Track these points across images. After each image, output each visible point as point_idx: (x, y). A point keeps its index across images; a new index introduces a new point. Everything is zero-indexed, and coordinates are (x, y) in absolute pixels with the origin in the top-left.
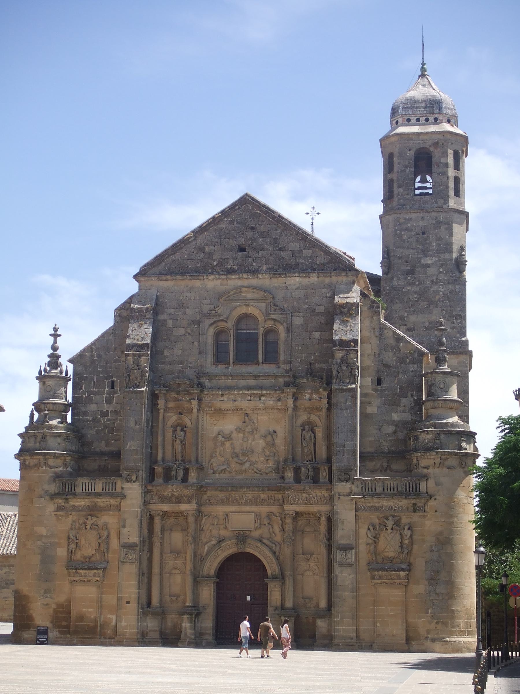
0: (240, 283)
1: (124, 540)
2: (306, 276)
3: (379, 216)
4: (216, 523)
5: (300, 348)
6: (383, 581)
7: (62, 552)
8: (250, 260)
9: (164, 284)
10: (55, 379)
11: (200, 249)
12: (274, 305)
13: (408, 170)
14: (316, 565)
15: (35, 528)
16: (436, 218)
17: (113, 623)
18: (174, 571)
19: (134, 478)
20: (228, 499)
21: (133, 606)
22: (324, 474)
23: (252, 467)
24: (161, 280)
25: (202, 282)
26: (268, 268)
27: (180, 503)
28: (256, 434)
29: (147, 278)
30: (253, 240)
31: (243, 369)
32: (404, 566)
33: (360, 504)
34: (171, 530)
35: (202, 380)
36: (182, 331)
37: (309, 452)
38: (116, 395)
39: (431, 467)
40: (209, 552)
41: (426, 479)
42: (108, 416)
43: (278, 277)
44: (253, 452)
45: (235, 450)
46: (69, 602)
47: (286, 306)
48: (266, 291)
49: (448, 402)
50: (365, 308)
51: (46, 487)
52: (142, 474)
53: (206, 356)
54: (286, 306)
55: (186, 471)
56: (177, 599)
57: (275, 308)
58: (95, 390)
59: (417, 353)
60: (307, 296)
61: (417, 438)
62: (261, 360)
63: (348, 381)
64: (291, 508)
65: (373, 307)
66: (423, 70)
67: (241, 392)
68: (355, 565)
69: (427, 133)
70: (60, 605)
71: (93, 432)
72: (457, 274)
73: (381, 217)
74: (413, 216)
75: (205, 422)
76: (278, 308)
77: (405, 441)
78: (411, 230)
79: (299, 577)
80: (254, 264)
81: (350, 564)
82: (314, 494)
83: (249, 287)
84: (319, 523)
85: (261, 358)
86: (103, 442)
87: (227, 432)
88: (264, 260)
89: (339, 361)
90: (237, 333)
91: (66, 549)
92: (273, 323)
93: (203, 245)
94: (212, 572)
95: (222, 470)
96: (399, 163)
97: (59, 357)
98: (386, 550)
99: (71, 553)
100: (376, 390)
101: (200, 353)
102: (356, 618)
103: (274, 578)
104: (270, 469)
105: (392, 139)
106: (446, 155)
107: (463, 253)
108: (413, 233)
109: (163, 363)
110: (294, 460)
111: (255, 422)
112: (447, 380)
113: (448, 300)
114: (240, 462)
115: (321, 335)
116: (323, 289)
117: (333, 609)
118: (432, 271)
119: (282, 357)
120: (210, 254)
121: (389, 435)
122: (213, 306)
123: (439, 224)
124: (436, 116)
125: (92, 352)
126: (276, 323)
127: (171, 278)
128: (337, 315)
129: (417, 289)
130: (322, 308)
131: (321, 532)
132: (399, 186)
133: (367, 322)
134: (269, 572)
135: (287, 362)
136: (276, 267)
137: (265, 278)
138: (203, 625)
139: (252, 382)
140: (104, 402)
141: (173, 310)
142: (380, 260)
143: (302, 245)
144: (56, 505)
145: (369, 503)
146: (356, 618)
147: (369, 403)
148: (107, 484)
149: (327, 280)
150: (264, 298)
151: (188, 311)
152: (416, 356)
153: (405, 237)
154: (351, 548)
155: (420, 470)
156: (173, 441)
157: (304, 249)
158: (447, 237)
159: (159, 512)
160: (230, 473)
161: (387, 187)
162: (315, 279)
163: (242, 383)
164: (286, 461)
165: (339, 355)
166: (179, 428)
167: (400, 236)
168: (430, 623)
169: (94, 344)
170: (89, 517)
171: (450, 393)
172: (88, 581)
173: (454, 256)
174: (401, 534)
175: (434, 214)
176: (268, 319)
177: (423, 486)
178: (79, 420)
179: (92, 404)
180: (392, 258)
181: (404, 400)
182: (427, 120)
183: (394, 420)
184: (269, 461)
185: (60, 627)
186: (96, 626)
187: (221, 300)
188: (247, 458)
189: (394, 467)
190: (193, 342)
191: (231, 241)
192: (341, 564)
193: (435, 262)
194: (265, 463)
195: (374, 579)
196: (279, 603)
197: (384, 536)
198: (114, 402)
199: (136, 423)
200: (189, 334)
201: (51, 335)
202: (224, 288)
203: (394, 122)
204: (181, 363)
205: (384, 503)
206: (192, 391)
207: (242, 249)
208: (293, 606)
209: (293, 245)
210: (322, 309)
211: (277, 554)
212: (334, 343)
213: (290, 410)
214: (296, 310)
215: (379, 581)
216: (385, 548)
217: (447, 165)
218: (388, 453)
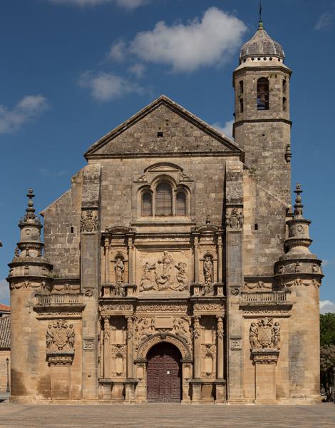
1: (85, 335)
7: (43, 344)
17: (80, 390)
21: (93, 379)
32: (275, 350)
51: (29, 300)
52: (96, 291)
55: (126, 288)
60: (206, 169)
62: (174, 213)
64: (197, 313)
70: (43, 379)
72: (285, 162)
78: (255, 134)
84: (217, 322)
86: (67, 270)
87: (151, 263)
94: (145, 356)
97: (33, 211)
99: (48, 344)
100: (254, 233)
101: (132, 208)
107: (289, 149)
109: (106, 215)
113: (280, 180)
118: (268, 161)
119: (189, 212)
123: (273, 129)
130: (217, 177)
134: (183, 355)
138: (139, 390)
139: (169, 229)
147: (249, 242)
149: (220, 158)
152: (281, 209)
154: (240, 339)
163: (162, 229)
165: (229, 211)
173: (284, 151)
178: (49, 255)
181: (273, 240)
182: (265, 59)
185: (43, 393)
186: (68, 392)
189: (266, 285)
192: (233, 349)
204: (119, 215)
207: (160, 135)
209: (196, 133)
214: (199, 178)
217: (279, 90)
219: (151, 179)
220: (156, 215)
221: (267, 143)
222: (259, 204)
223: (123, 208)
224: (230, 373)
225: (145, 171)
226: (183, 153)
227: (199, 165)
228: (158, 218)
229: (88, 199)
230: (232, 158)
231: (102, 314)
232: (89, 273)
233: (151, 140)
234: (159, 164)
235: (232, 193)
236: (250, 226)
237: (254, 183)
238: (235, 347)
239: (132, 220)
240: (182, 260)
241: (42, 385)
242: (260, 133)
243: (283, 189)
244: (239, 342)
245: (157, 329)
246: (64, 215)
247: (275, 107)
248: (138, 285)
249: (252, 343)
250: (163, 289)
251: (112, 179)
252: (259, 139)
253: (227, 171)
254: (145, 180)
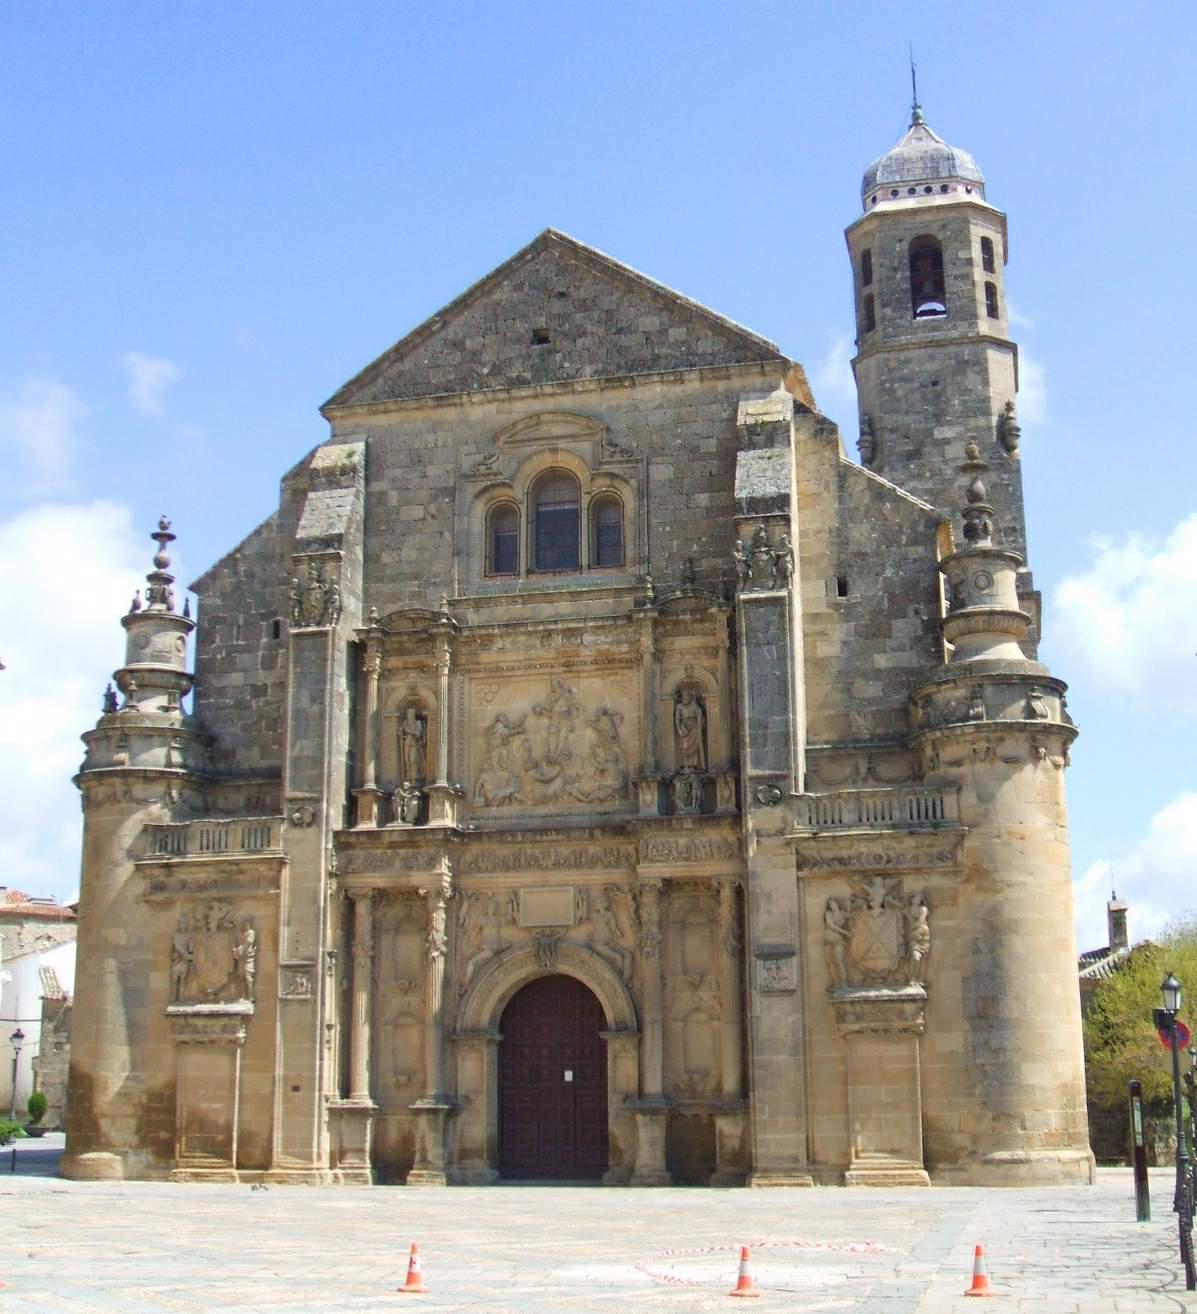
0: (536, 406)
2: (674, 382)
3: (852, 361)
4: (491, 912)
5: (668, 529)
6: (864, 1025)
8: (558, 357)
9: (382, 420)
10: (156, 621)
11: (455, 345)
12: (611, 444)
13: (899, 276)
14: (715, 997)
15: (104, 931)
16: (957, 355)
17: (265, 1136)
18: (403, 1020)
19: (308, 819)
20: (517, 858)
22: (724, 793)
23: (568, 788)
24: (375, 413)
25: (458, 409)
26: (595, 372)
27: (411, 868)
28: (577, 716)
29: (346, 412)
30: (563, 317)
31: (547, 582)
33: (807, 853)
34: (397, 931)
35: (459, 611)
36: (419, 512)
37: (694, 748)
38: (281, 651)
39: (967, 761)
41: (954, 789)
42: (265, 695)
43: (618, 387)
44: (570, 756)
45: (534, 754)
46: (172, 1086)
47: (635, 444)
48: (590, 417)
49: (998, 617)
50: (804, 436)
54: (635, 444)
56: (409, 1079)
57: (613, 449)
58: (241, 643)
59: (923, 521)
60: (679, 421)
61: (928, 700)
62: (584, 561)
63: (771, 584)
64: (653, 871)
65: (822, 430)
66: (916, 117)
67: (541, 628)
68: (799, 992)
69: (930, 209)
70: (154, 1096)
71: (236, 729)
73: (854, 363)
74: (915, 354)
75: (466, 697)
76: (618, 449)
77: (905, 712)
78: (912, 380)
79: (677, 1026)
80: (566, 365)
81: (789, 991)
82: (704, 839)
83: (554, 413)
84: (719, 904)
85: (584, 558)
86: (256, 751)
87: (514, 717)
88: (586, 354)
89: (750, 543)
90: (538, 514)
91: (167, 974)
92: (608, 481)
93: (460, 335)
94: (485, 1018)
95: (504, 798)
96: (881, 265)
97: (169, 580)
98: (871, 955)
100: (837, 606)
102: (805, 1112)
103: (622, 1028)
104: (610, 791)
105: (867, 227)
106: (967, 243)
107: (1011, 414)
108: (916, 385)
110: (658, 767)
112: (991, 569)
114: (541, 778)
115: (711, 499)
116: (714, 403)
117: (751, 1094)
119: (630, 552)
120: (475, 355)
121: (871, 701)
122: (482, 456)
124: (945, 182)
125: (235, 566)
126: (617, 483)
127: (392, 407)
128: (742, 449)
129: (930, 485)
130: (713, 442)
131: (723, 922)
132: (885, 305)
133: (812, 463)
134: (610, 1016)
135: (641, 560)
136: (612, 368)
137: (590, 391)
139: (565, 607)
140: (259, 666)
141: (400, 471)
142: (857, 436)
143: (666, 320)
144: (148, 881)
145: (829, 849)
146: (807, 1113)
148: (252, 832)
149: (721, 386)
150: (588, 432)
151: (432, 471)
152: (921, 528)
153: (900, 393)
154: (791, 954)
155: (942, 771)
156: (399, 740)
157: (671, 327)
158: (980, 387)
159: (366, 890)
160: (521, 802)
161: (863, 311)
162: (697, 385)
163: (546, 610)
164: (641, 770)
165: (748, 530)
166: (411, 713)
167: (892, 391)
168: (979, 1118)
169: (238, 550)
170: (215, 904)
171: (1000, 598)
172: (212, 1042)
174: (905, 918)
175: (952, 349)
176: (598, 474)
177: (950, 800)
178: (208, 706)
179: (235, 671)
180: (878, 433)
181: (898, 624)
183: (879, 670)
184: (606, 773)
187: (500, 443)
188: (557, 768)
189: (884, 770)
190: (441, 533)
191: (518, 324)
192: (768, 992)
193: (960, 433)
195: (844, 1021)
196: (633, 1086)
197: (864, 922)
198: (279, 664)
199: (313, 700)
200: (433, 517)
201: (155, 536)
202: (503, 419)
203: (869, 200)
204: (416, 576)
205: (863, 849)
206: (435, 630)
207: (540, 338)
210: (712, 445)
211: (627, 974)
212: (735, 506)
213: (647, 658)
214: (658, 451)
215: (856, 1027)
216: (868, 951)
217: (970, 262)
218: (871, 740)
219: (514, 465)
220: (529, 572)
221: (947, 402)
222: (847, 515)
223: (427, 555)
224: (757, 1073)
225: (495, 439)
226: (607, 380)
227: (658, 414)
228: (533, 578)
229: (316, 532)
230: (757, 381)
231: (353, 881)
232: (306, 753)
233: (517, 352)
234: (535, 418)
235: (753, 476)
236: (822, 583)
237: (828, 454)
238: (776, 985)
240: (608, 705)
241: (154, 1116)
242: (924, 378)
243: (1001, 526)
244: (790, 970)
245: (528, 929)
246: (257, 585)
247: (962, 307)
248: (469, 786)
249: (831, 962)
250: (544, 800)
251: (398, 472)
252: (925, 394)
253: (741, 420)
254: (495, 467)
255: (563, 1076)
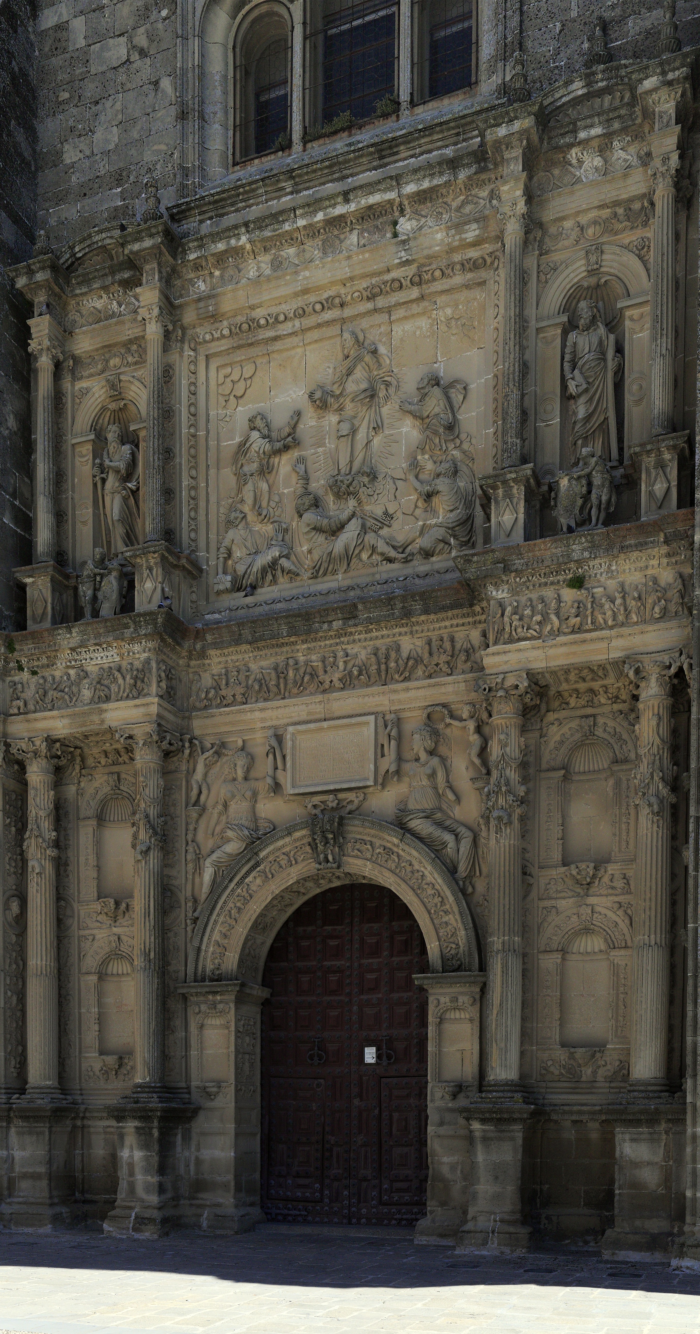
27: (108, 699)
28: (387, 398)
40: (217, 888)
53: (201, 128)
111: (382, 350)
194: (418, 512)
196: (470, 1070)
208: (522, 1076)
239: (183, 190)
255: (379, 1057)
